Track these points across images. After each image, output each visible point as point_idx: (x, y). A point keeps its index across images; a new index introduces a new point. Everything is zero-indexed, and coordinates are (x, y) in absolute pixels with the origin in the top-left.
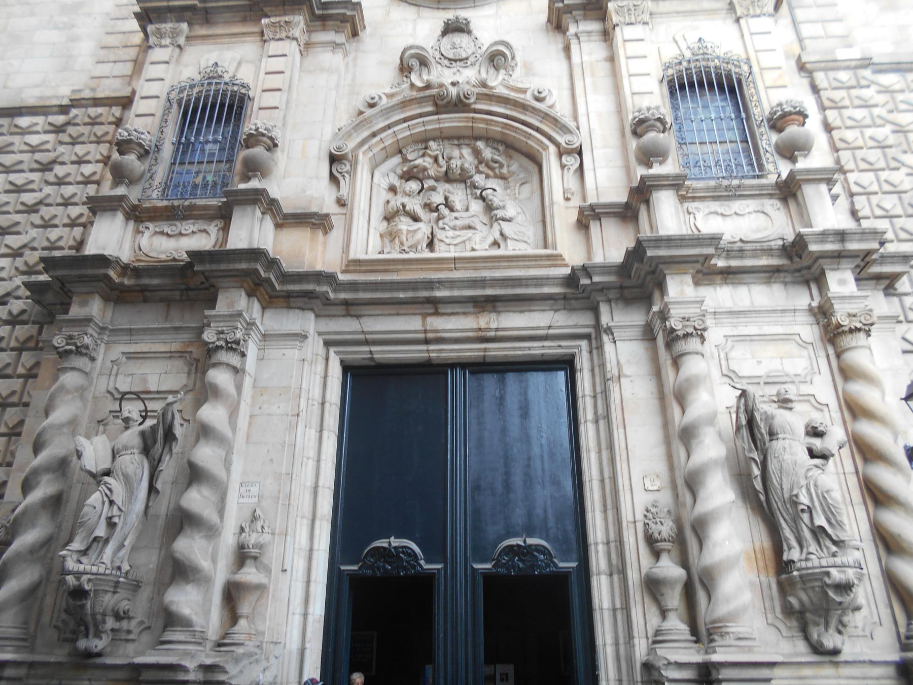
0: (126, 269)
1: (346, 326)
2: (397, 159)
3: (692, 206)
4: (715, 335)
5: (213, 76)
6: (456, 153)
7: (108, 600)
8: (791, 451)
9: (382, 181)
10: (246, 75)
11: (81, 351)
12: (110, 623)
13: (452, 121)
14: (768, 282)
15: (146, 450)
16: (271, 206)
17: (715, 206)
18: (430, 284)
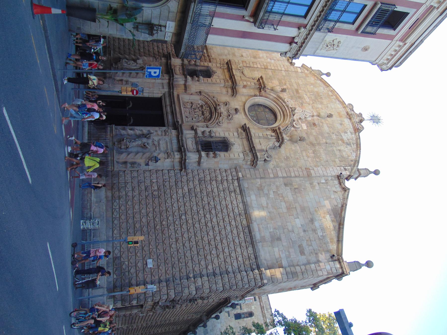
0: (170, 63)
1: (167, 95)
2: (204, 104)
3: (194, 139)
4: (167, 138)
5: (215, 72)
6: (208, 113)
7: (119, 65)
8: (145, 140)
9: (200, 102)
10: (214, 77)
11: (156, 60)
12: (116, 66)
13: (213, 109)
14: (178, 148)
15: (141, 67)
16: (186, 81)
17: (194, 142)
18: (174, 103)
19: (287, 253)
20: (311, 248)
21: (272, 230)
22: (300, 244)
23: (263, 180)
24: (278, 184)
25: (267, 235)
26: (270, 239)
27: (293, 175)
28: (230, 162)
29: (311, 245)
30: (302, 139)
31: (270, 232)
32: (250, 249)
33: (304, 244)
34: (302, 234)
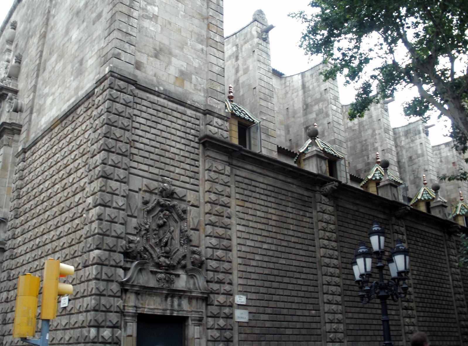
19: (96, 42)
20: (99, 3)
21: (72, 78)
22: (92, 23)
23: (34, 110)
24: (41, 82)
25: (74, 84)
26: (79, 78)
27: (38, 62)
28: (9, 169)
29: (97, 4)
30: (19, 60)
31: (74, 80)
32: (79, 110)
33: (94, 15)
34: (85, 24)
